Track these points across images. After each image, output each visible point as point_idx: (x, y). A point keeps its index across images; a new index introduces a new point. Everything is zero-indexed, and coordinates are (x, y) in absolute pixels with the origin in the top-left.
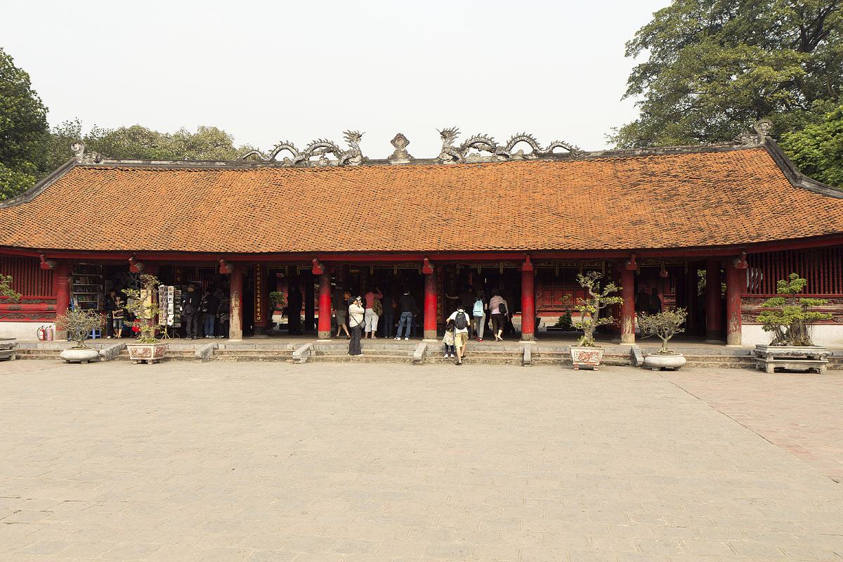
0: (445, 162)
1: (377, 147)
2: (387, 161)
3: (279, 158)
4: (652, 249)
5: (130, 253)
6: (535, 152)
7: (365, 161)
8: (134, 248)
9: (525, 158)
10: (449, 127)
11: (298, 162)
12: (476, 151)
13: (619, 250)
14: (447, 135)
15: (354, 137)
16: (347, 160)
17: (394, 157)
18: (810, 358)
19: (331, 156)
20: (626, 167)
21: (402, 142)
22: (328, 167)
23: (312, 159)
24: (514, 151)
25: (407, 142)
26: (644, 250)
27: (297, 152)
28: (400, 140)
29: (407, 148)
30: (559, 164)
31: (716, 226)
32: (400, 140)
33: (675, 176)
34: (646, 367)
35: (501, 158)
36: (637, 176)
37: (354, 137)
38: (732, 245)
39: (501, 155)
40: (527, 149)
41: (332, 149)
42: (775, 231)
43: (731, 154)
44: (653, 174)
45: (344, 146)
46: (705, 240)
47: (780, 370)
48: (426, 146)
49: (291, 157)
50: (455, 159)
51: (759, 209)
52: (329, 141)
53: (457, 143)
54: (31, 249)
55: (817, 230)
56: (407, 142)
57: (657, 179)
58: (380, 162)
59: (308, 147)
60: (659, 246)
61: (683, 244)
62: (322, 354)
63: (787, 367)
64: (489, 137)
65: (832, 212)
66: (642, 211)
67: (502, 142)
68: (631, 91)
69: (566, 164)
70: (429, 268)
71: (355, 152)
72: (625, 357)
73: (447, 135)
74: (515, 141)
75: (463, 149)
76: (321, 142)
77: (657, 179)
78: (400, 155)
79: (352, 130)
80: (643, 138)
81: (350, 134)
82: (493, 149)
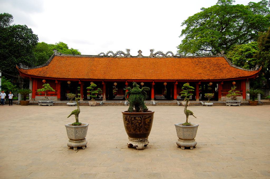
1: (134, 53)
2: (136, 57)
3: (109, 55)
4: (204, 80)
5: (79, 79)
6: (172, 56)
7: (131, 56)
8: (81, 78)
9: (170, 57)
10: (152, 49)
11: (114, 56)
12: (158, 55)
13: (197, 80)
14: (152, 51)
15: (128, 50)
17: (138, 56)
18: (237, 103)
19: (122, 55)
21: (140, 52)
22: (122, 58)
23: (117, 55)
24: (167, 55)
25: (142, 52)
26: (203, 80)
28: (140, 52)
29: (142, 53)
30: (178, 59)
31: (217, 75)
32: (140, 52)
34: (204, 105)
35: (164, 57)
36: (197, 63)
37: (128, 50)
38: (221, 79)
40: (171, 55)
43: (216, 58)
44: (200, 62)
45: (126, 53)
46: (215, 78)
48: (146, 53)
49: (112, 55)
50: (154, 57)
51: (225, 71)
53: (154, 53)
54: (54, 78)
56: (142, 52)
57: (202, 63)
58: (135, 57)
64: (162, 52)
65: (240, 72)
66: (200, 71)
67: (165, 53)
68: (182, 35)
70: (153, 84)
71: (129, 54)
72: (199, 104)
73: (152, 51)
74: (168, 53)
75: (156, 54)
77: (202, 63)
79: (128, 49)
80: (185, 47)
82: (163, 54)
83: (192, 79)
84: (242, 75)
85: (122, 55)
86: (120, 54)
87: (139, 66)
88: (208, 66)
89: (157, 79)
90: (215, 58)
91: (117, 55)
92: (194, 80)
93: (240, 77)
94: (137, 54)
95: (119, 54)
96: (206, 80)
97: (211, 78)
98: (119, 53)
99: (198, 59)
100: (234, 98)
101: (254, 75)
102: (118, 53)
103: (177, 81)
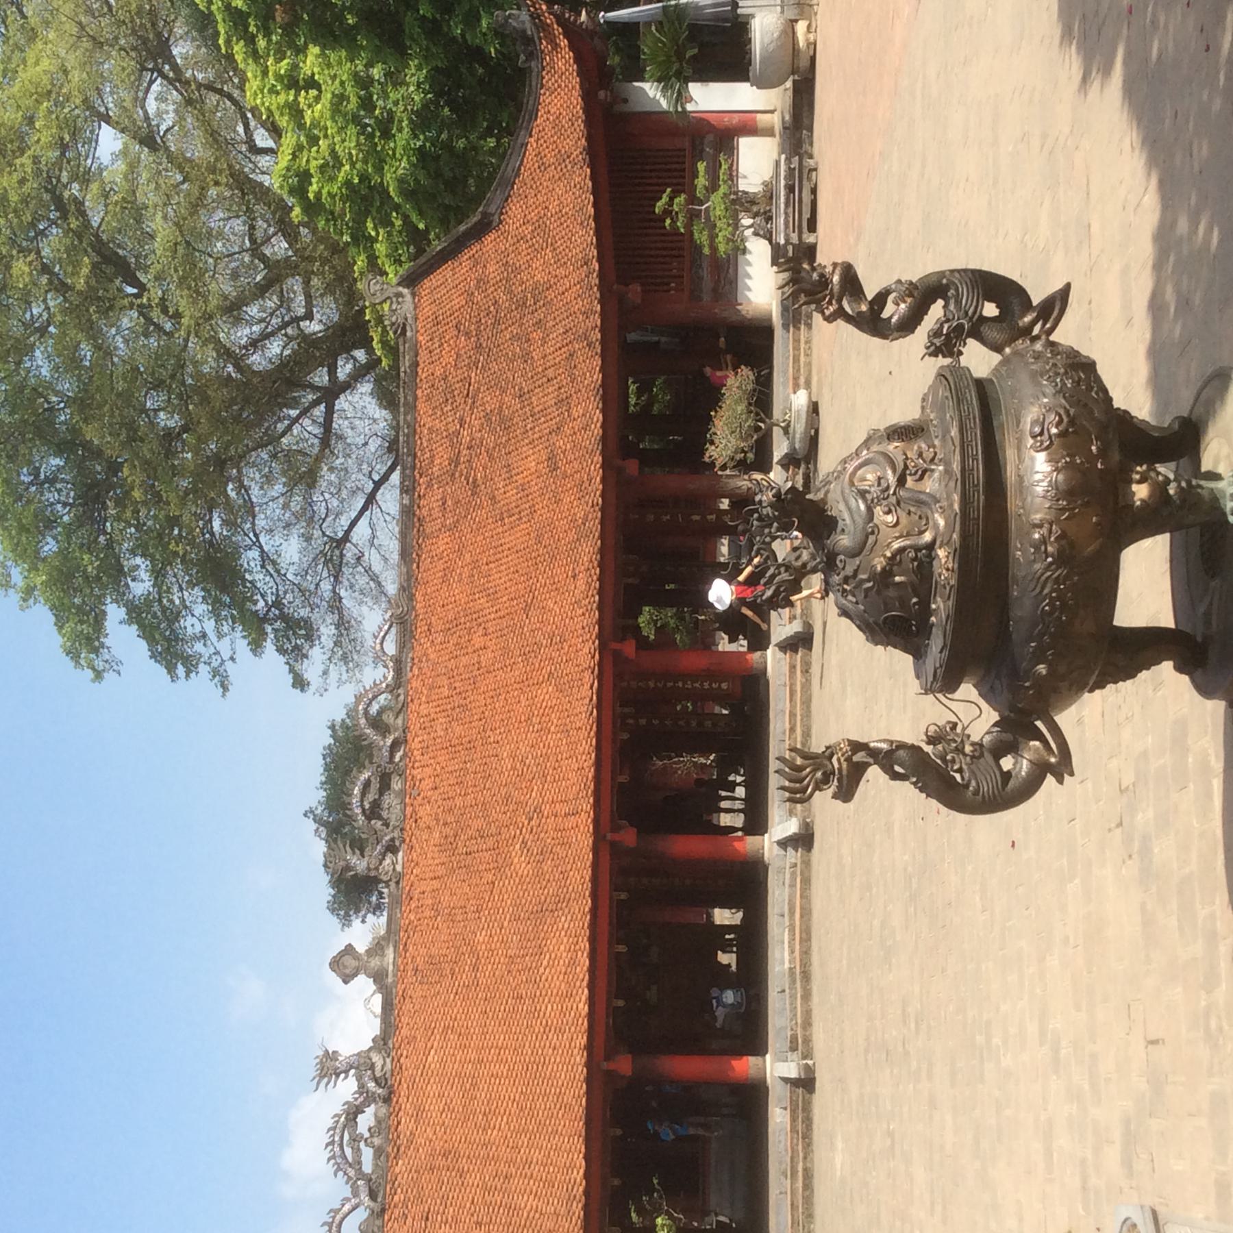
0: (399, 868)
7: (383, 1042)
11: (373, 1195)
15: (329, 1067)
16: (376, 1080)
17: (379, 977)
19: (366, 1121)
20: (436, 513)
21: (350, 962)
23: (367, 1167)
27: (348, 1200)
33: (462, 422)
39: (392, 756)
41: (353, 1113)
42: (581, 240)
45: (347, 1088)
47: (812, 227)
49: (361, 1215)
52: (330, 1123)
55: (581, 176)
56: (349, 950)
59: (341, 1174)
60: (598, 416)
61: (598, 377)
62: (794, 1040)
63: (806, 215)
66: (531, 461)
69: (422, 627)
71: (361, 1065)
76: (333, 1157)
78: (375, 963)
79: (312, 1071)
81: (322, 1077)
83: (594, 525)
84: (574, 140)
85: (366, 1121)
86: (355, 1139)
87: (475, 968)
88: (489, 401)
89: (587, 804)
90: (423, 357)
91: (367, 1167)
92: (603, 510)
93: (592, 152)
94: (364, 984)
95: (357, 1152)
96: (603, 411)
97: (590, 371)
98: (348, 1152)
99: (429, 485)
100: (759, 206)
101: (572, 47)
102: (344, 1164)
103: (615, 646)
